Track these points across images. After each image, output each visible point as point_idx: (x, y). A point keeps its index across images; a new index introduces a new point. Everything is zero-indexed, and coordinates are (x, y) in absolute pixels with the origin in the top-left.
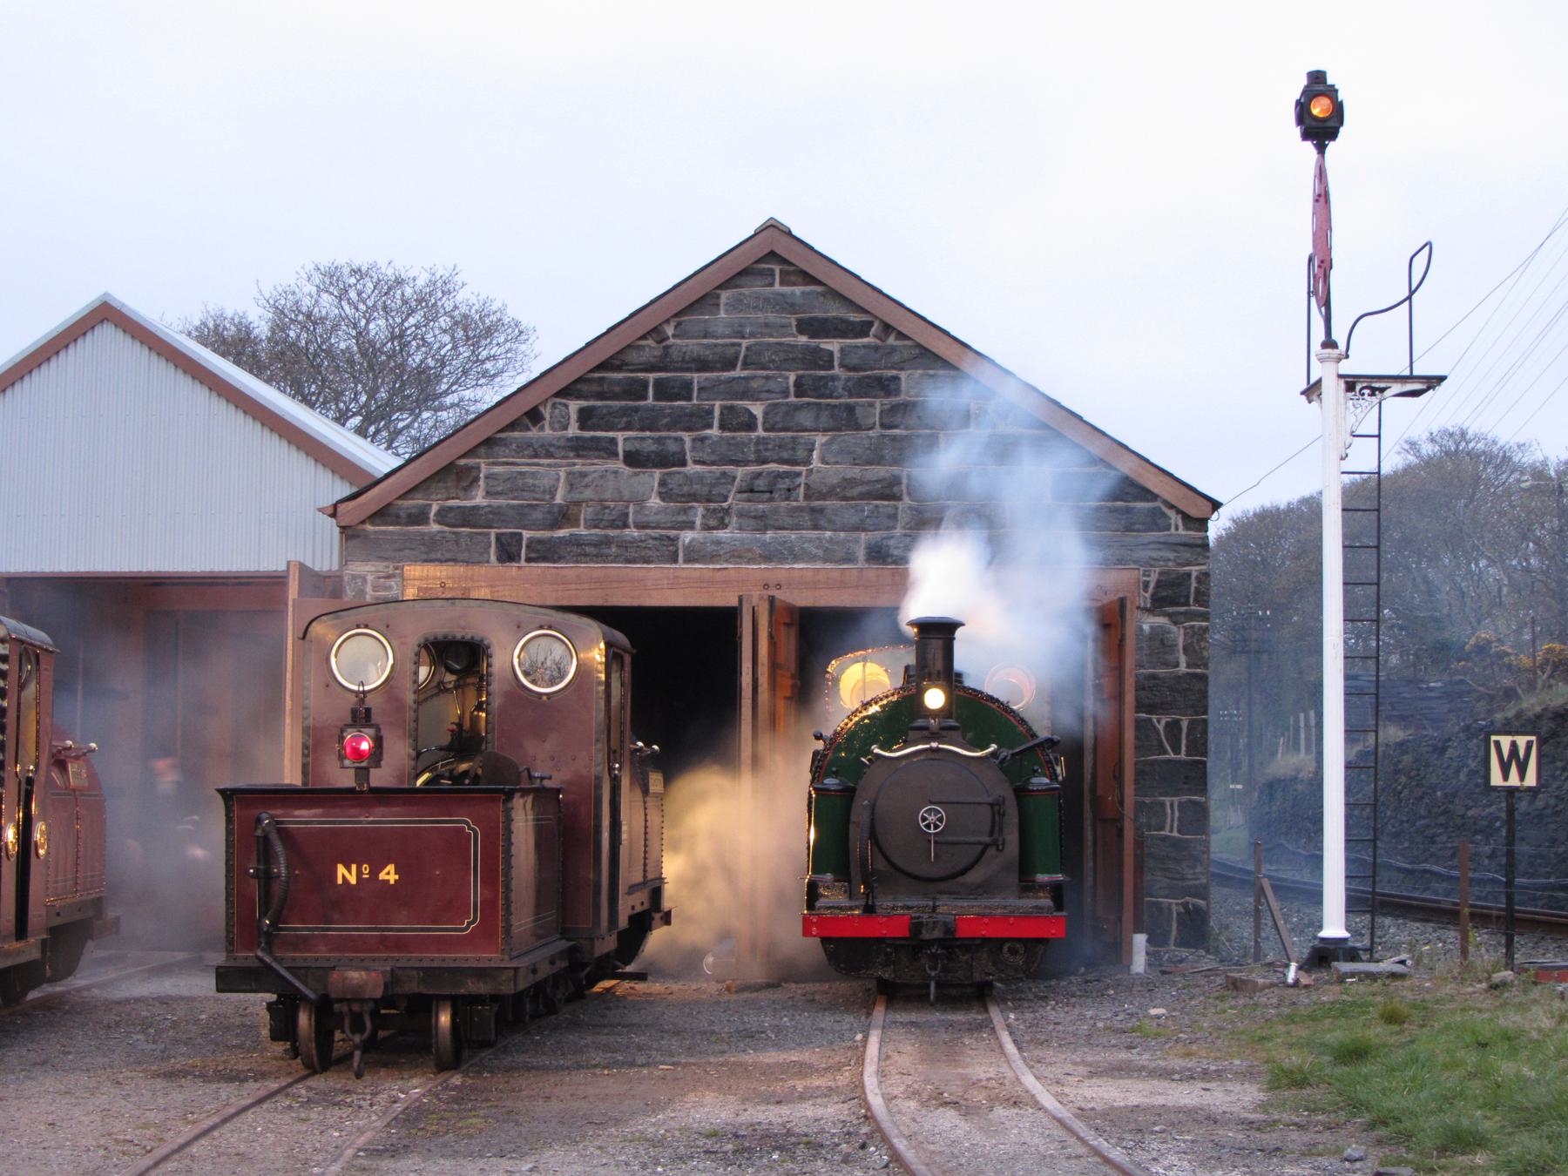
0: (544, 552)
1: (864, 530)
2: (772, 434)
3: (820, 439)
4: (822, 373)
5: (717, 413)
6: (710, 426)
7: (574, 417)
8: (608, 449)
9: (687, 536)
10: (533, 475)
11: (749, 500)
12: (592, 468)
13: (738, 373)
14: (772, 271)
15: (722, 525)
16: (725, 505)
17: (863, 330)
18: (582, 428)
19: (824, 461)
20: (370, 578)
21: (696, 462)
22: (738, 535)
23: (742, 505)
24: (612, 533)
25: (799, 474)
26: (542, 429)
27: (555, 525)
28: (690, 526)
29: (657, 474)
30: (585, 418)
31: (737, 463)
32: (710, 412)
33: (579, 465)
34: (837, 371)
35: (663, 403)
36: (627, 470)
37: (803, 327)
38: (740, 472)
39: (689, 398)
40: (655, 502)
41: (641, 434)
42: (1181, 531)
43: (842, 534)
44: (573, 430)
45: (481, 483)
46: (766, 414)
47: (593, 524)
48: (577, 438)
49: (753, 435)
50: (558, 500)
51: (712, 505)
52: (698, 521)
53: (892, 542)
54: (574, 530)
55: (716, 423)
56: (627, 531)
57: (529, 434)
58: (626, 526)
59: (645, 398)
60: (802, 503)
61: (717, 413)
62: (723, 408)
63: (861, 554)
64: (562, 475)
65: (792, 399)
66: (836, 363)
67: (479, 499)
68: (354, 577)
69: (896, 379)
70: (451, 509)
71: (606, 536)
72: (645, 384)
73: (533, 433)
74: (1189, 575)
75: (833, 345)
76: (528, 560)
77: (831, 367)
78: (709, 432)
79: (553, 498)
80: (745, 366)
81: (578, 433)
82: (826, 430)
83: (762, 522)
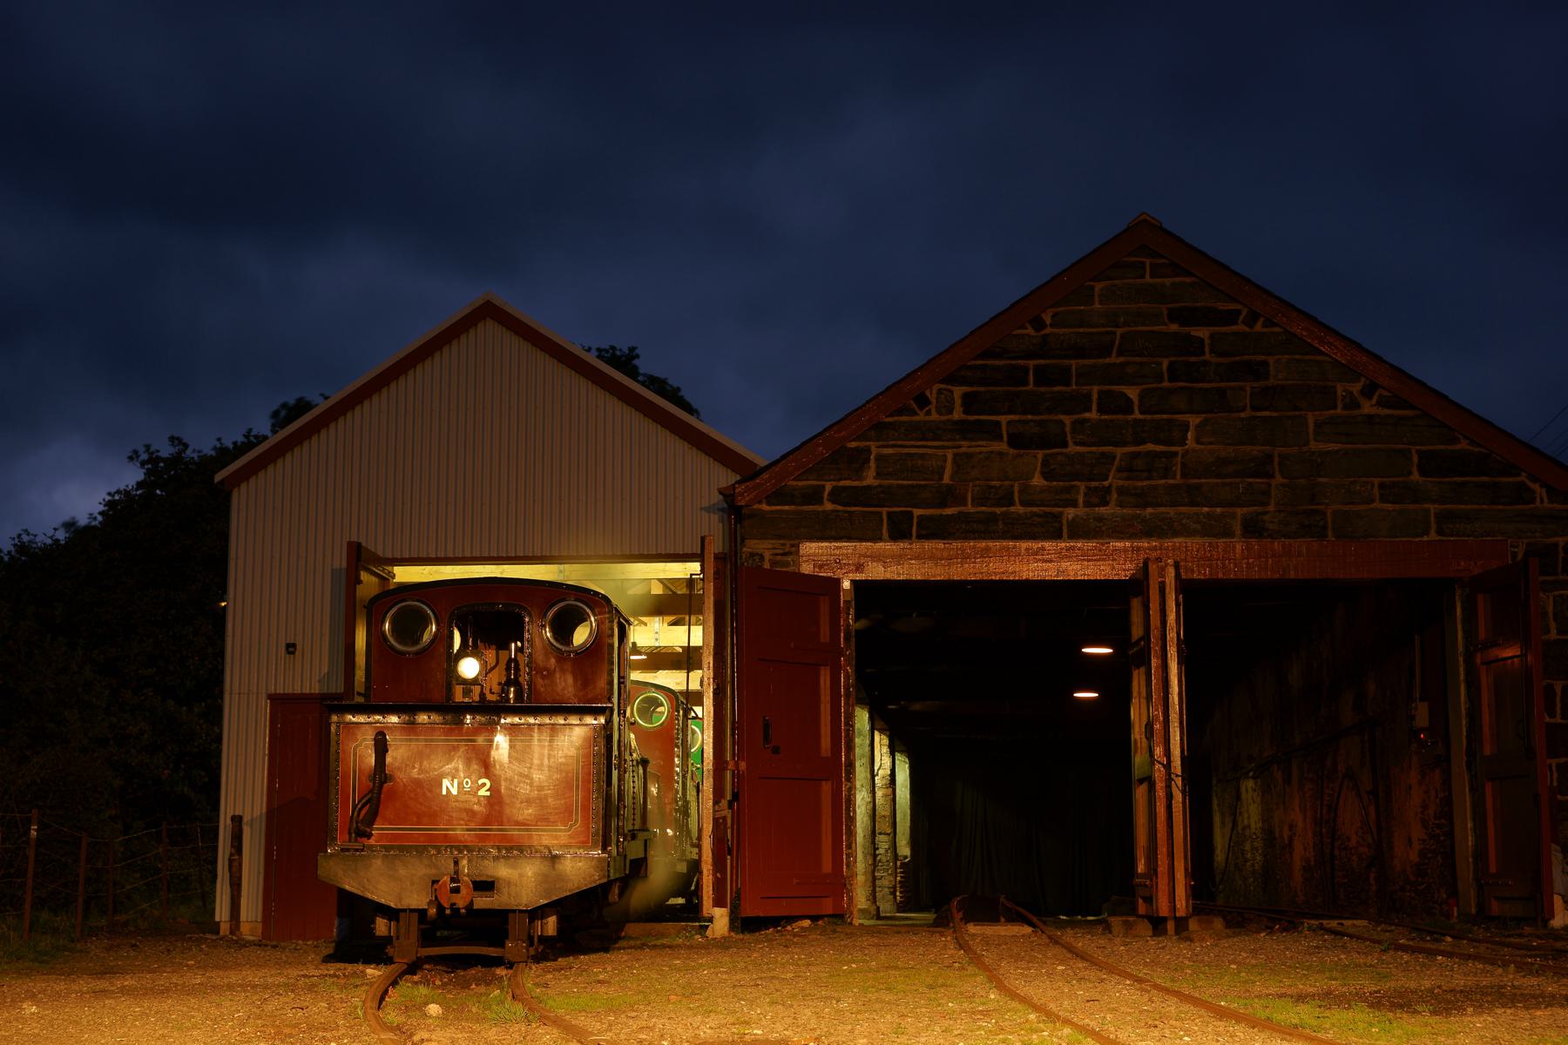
0: (934, 530)
1: (1240, 506)
2: (1148, 417)
3: (1194, 420)
4: (1193, 359)
5: (1095, 397)
6: (1089, 410)
7: (958, 402)
8: (993, 432)
9: (1070, 513)
10: (922, 456)
11: (1128, 479)
12: (978, 450)
13: (1114, 359)
14: (1143, 264)
15: (1105, 504)
16: (1106, 483)
17: (1231, 317)
18: (965, 412)
19: (1198, 442)
20: (767, 555)
21: (1076, 444)
22: (1118, 510)
23: (1121, 483)
24: (998, 510)
25: (1176, 454)
26: (928, 413)
27: (943, 505)
28: (1074, 504)
29: (1040, 454)
30: (969, 403)
31: (1116, 444)
32: (1088, 396)
33: (965, 447)
34: (1207, 357)
35: (1042, 389)
36: (1012, 451)
37: (1174, 316)
38: (1119, 451)
39: (1068, 384)
40: (1037, 481)
41: (1023, 417)
42: (1546, 504)
43: (1219, 510)
44: (958, 414)
45: (872, 464)
46: (1141, 397)
47: (980, 500)
48: (962, 422)
49: (1130, 417)
50: (946, 480)
51: (1094, 484)
52: (1081, 501)
53: (1266, 518)
54: (962, 509)
55: (1094, 407)
56: (1012, 509)
57: (917, 418)
58: (1012, 504)
59: (1027, 384)
60: (1178, 480)
61: (1095, 397)
62: (1100, 392)
63: (1238, 529)
64: (950, 457)
65: (1166, 384)
66: (1207, 349)
67: (870, 479)
68: (752, 555)
69: (1265, 363)
70: (845, 488)
71: (994, 514)
72: (1026, 370)
73: (921, 417)
74: (1556, 545)
75: (1202, 333)
76: (920, 537)
77: (1203, 353)
78: (1087, 415)
79: (941, 478)
80: (1120, 354)
81: (963, 417)
82: (1198, 413)
83: (1143, 499)
